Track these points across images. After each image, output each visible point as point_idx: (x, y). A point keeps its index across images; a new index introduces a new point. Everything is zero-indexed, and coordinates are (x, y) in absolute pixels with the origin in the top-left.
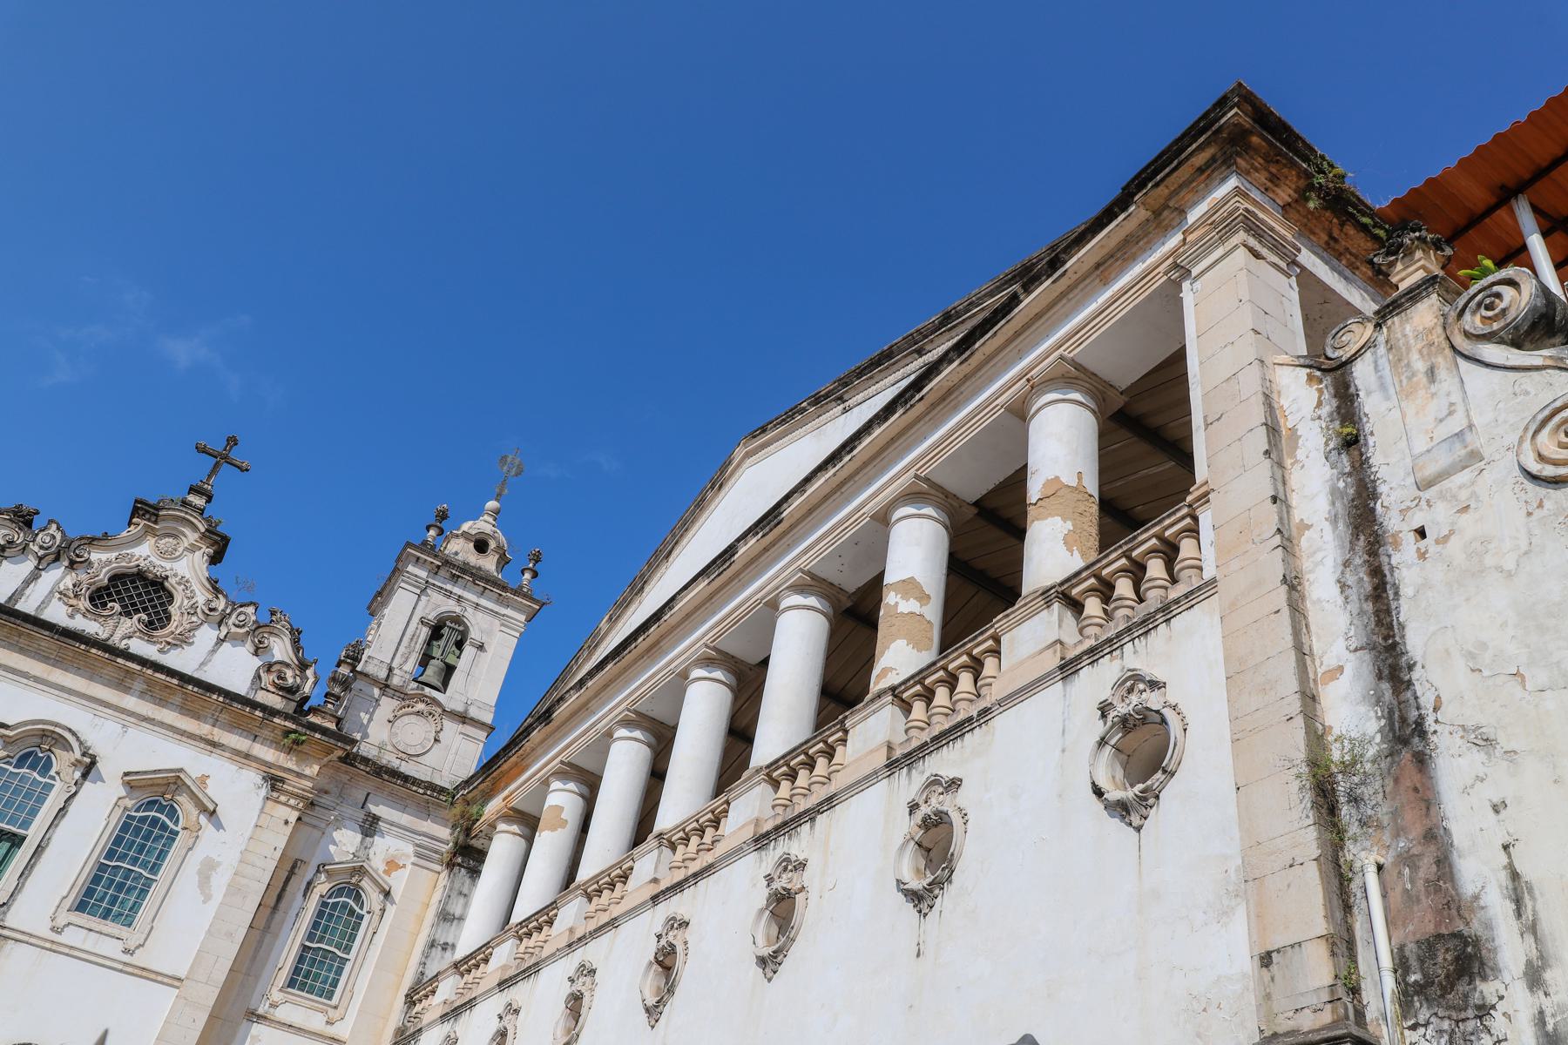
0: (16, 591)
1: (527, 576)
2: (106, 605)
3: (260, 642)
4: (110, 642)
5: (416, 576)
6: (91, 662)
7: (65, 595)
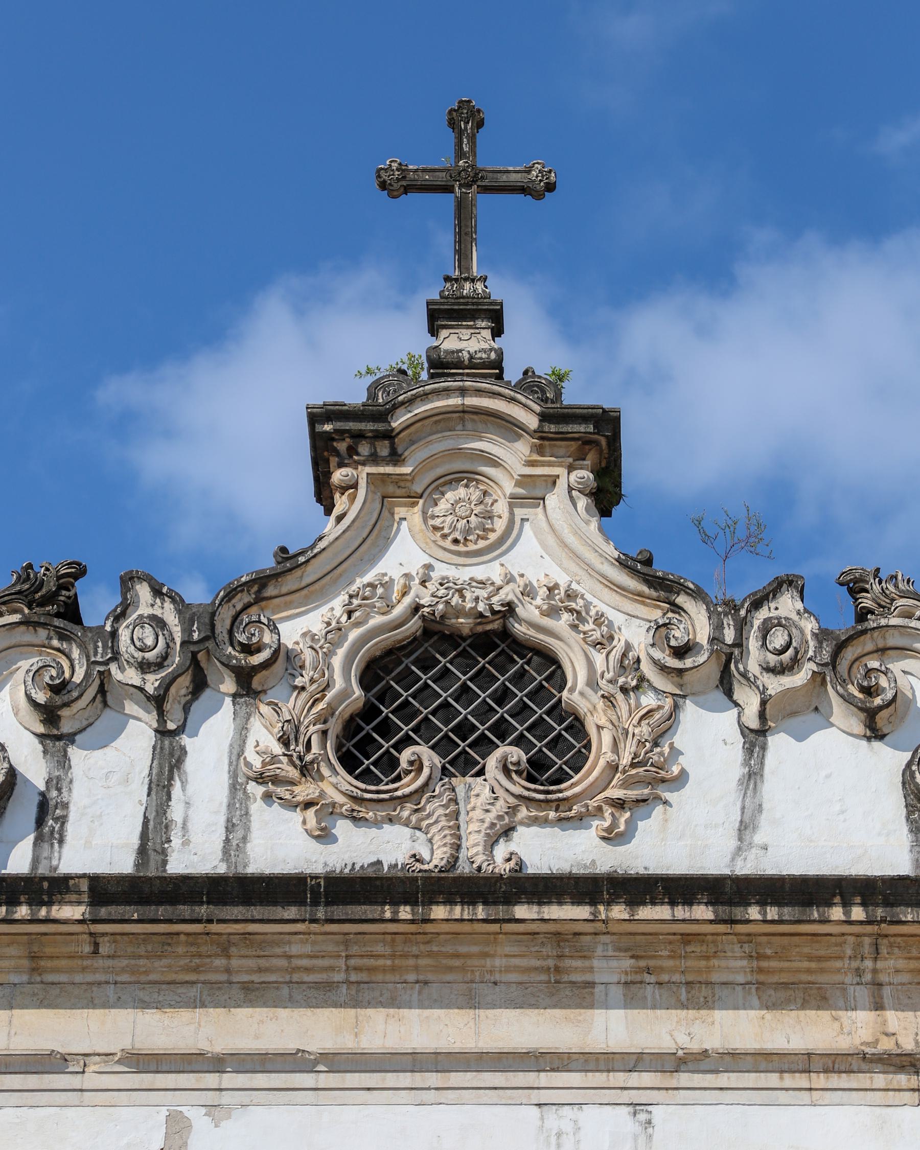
0: (146, 821)
2: (395, 763)
3: (869, 691)
4: (463, 868)
6: (449, 949)
7: (276, 780)
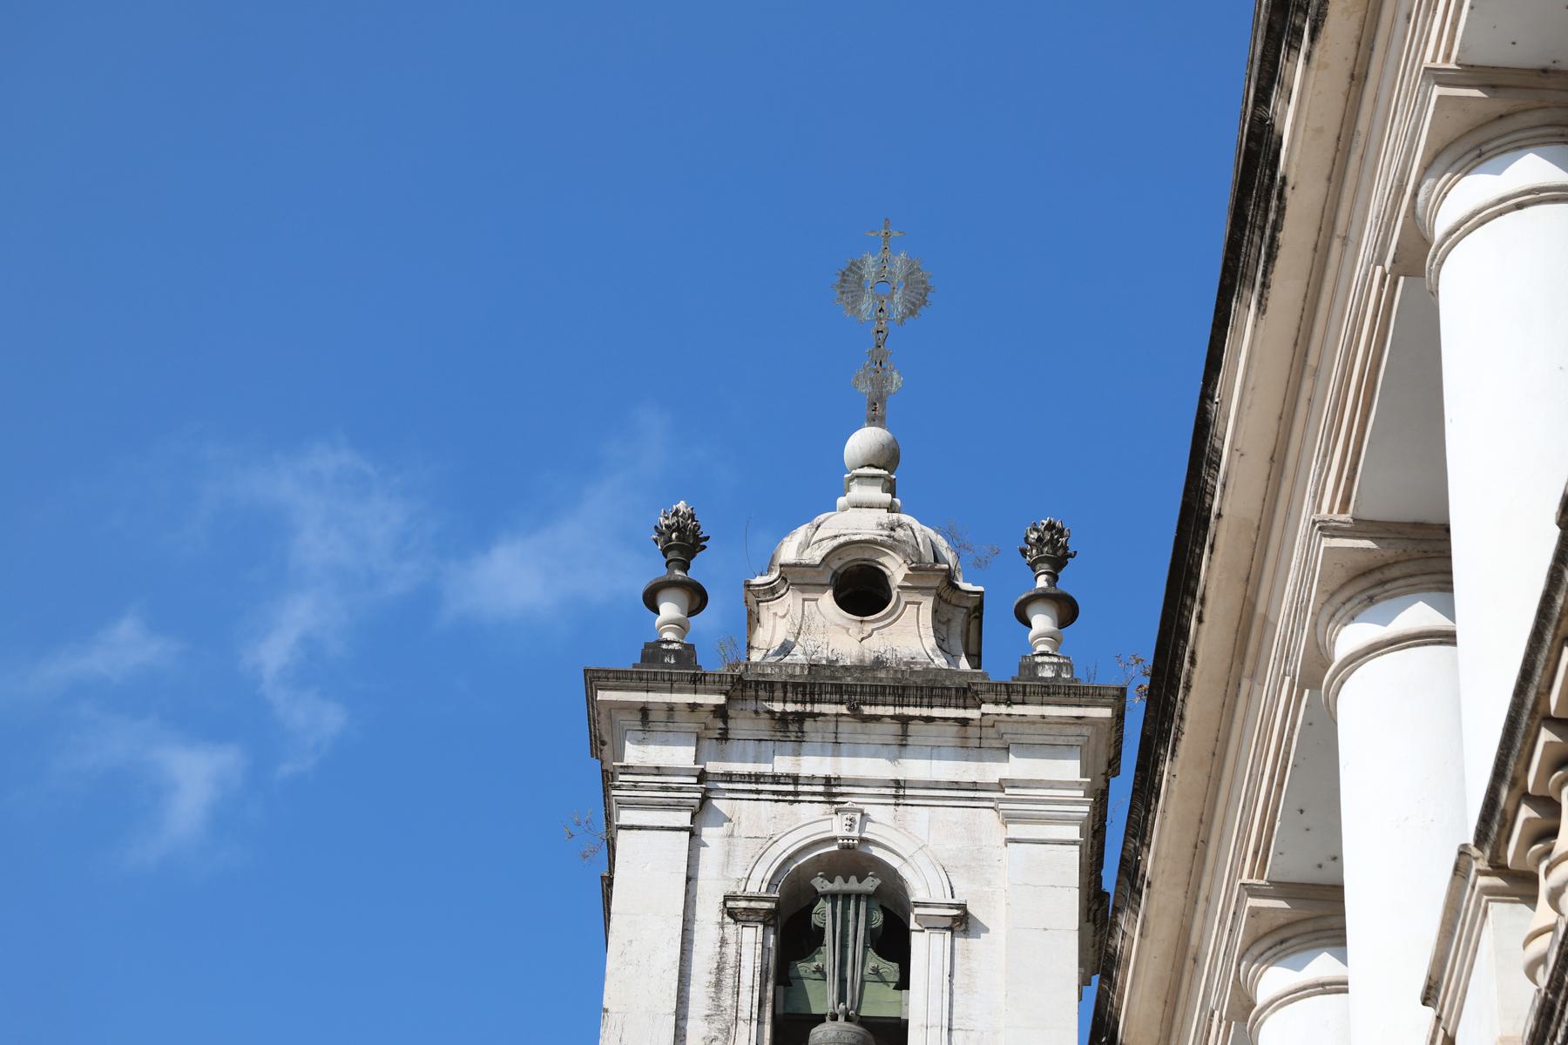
1: (1042, 622)
5: (659, 771)
